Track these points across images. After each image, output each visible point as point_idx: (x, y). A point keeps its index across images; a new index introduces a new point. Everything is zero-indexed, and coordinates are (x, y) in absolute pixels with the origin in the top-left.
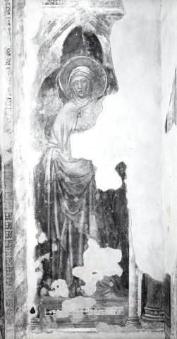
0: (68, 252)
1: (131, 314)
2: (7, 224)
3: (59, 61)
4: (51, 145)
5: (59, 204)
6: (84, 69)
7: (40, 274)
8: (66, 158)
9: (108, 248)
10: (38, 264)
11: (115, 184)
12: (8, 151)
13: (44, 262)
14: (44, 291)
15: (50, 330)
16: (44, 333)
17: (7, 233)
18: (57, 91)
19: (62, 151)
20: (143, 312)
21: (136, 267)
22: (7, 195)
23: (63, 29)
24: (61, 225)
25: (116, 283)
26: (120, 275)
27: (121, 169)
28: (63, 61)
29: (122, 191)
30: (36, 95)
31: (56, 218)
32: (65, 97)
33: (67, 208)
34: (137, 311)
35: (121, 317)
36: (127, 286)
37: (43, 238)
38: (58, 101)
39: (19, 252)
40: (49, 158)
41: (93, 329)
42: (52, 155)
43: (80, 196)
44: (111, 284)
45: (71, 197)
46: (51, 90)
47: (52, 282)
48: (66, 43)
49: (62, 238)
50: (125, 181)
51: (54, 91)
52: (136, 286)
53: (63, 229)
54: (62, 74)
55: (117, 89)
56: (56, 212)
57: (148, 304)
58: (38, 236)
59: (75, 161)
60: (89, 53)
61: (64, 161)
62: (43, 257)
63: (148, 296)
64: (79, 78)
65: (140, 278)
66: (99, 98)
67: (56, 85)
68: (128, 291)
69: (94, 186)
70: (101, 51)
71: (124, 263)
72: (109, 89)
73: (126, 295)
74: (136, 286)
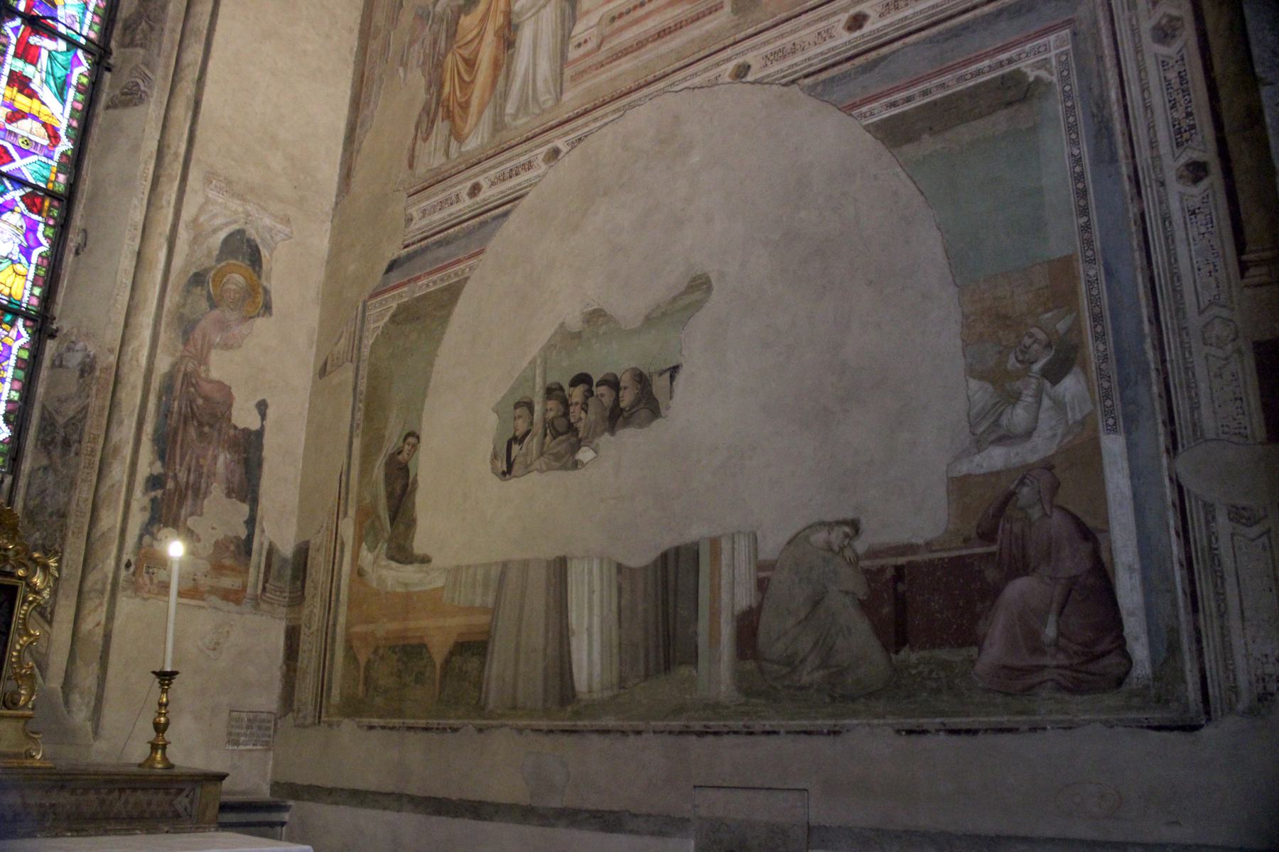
0: (186, 495)
1: (249, 591)
2: (89, 449)
3: (214, 259)
4: (186, 353)
5: (185, 429)
6: (238, 278)
7: (147, 515)
8: (203, 375)
9: (234, 500)
10: (146, 501)
11: (253, 423)
12: (109, 350)
13: (153, 500)
14: (147, 539)
15: (146, 596)
16: (138, 600)
17: (87, 461)
18: (205, 293)
19: (200, 364)
20: (264, 589)
21: (263, 531)
22: (97, 409)
23: (226, 224)
24: (183, 458)
25: (238, 546)
26: (243, 537)
27: (262, 407)
28: (219, 260)
29: (260, 433)
30: (180, 288)
31: (178, 446)
32: (213, 306)
33: (195, 437)
34: (257, 587)
35: (236, 592)
36: (249, 553)
37: (158, 468)
38: (204, 305)
39: (113, 486)
40: (183, 369)
41: (201, 603)
42: (190, 366)
43: (211, 426)
44: (232, 548)
45: (201, 424)
46: (199, 288)
47: (159, 530)
48: (226, 241)
49: (182, 476)
50: (264, 423)
51: (202, 290)
52: (260, 555)
53: (185, 463)
54: (215, 275)
55: (271, 314)
56: (179, 439)
57: (271, 580)
58: (151, 464)
59: (211, 382)
60: (248, 263)
61: (200, 377)
62: (153, 494)
63: (272, 570)
64: (233, 287)
65: (266, 546)
66: (250, 318)
67: (206, 285)
68: (250, 560)
69: (230, 420)
70: (261, 267)
71: (251, 522)
72: (262, 311)
73: (247, 566)
74: (260, 555)
